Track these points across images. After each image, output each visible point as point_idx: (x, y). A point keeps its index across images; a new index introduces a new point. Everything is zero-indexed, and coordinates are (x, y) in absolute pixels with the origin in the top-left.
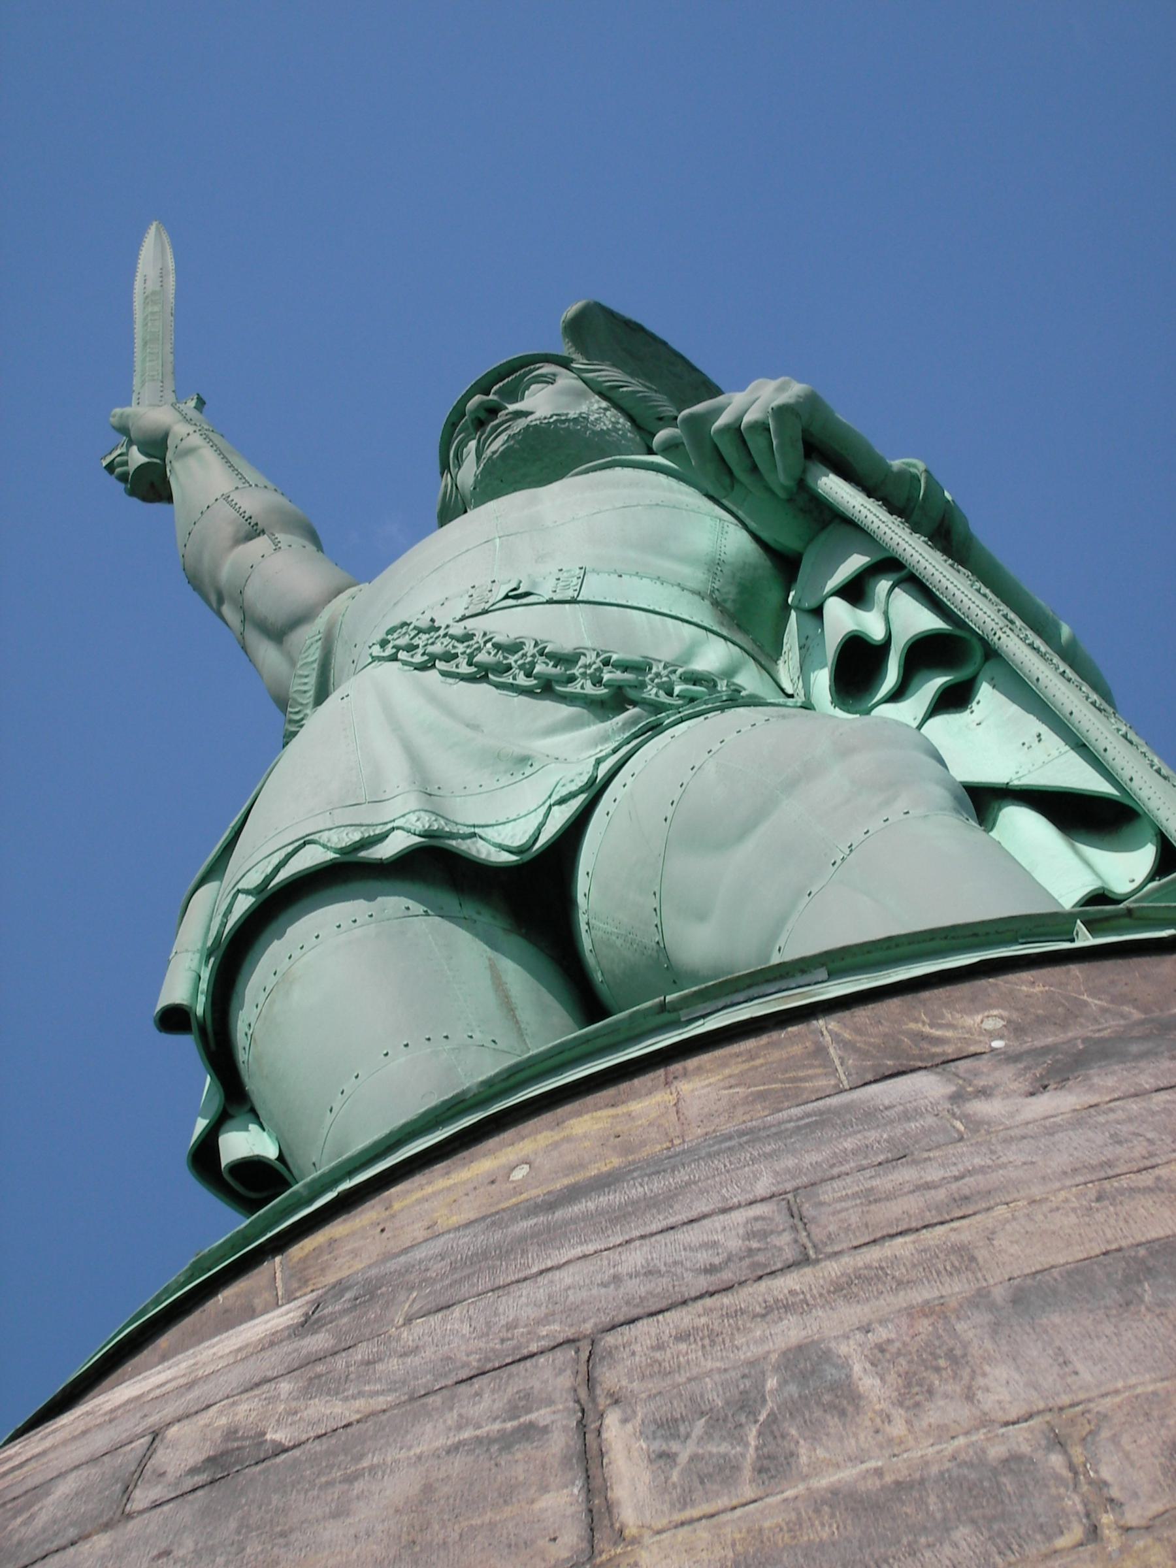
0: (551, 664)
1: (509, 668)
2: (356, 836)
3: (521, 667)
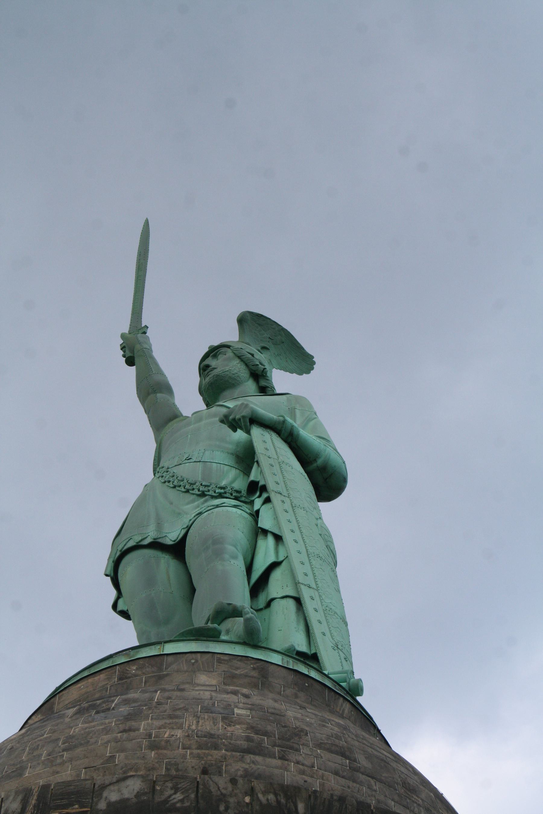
0: (189, 485)
2: (140, 539)
3: (183, 486)
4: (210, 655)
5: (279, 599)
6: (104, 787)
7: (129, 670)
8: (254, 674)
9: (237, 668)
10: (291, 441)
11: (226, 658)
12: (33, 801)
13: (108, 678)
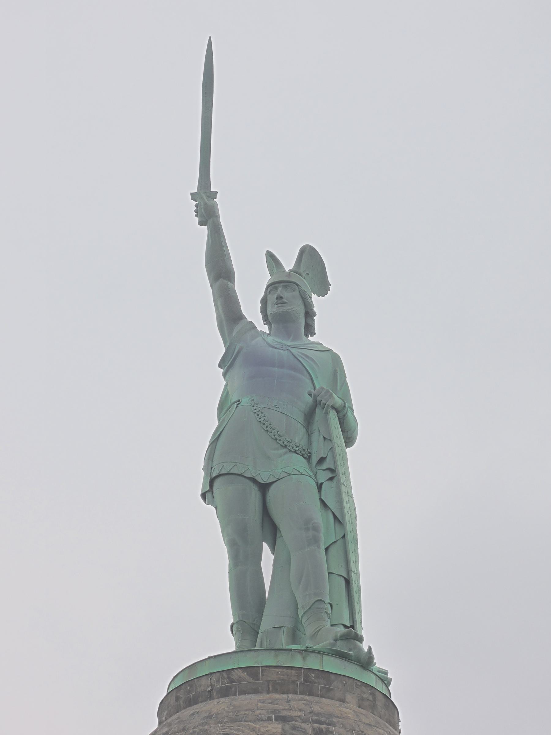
1: (271, 433)
4: (352, 679)
5: (336, 575)
7: (310, 675)
8: (371, 698)
9: (364, 693)
10: (342, 418)
11: (359, 683)
13: (297, 675)
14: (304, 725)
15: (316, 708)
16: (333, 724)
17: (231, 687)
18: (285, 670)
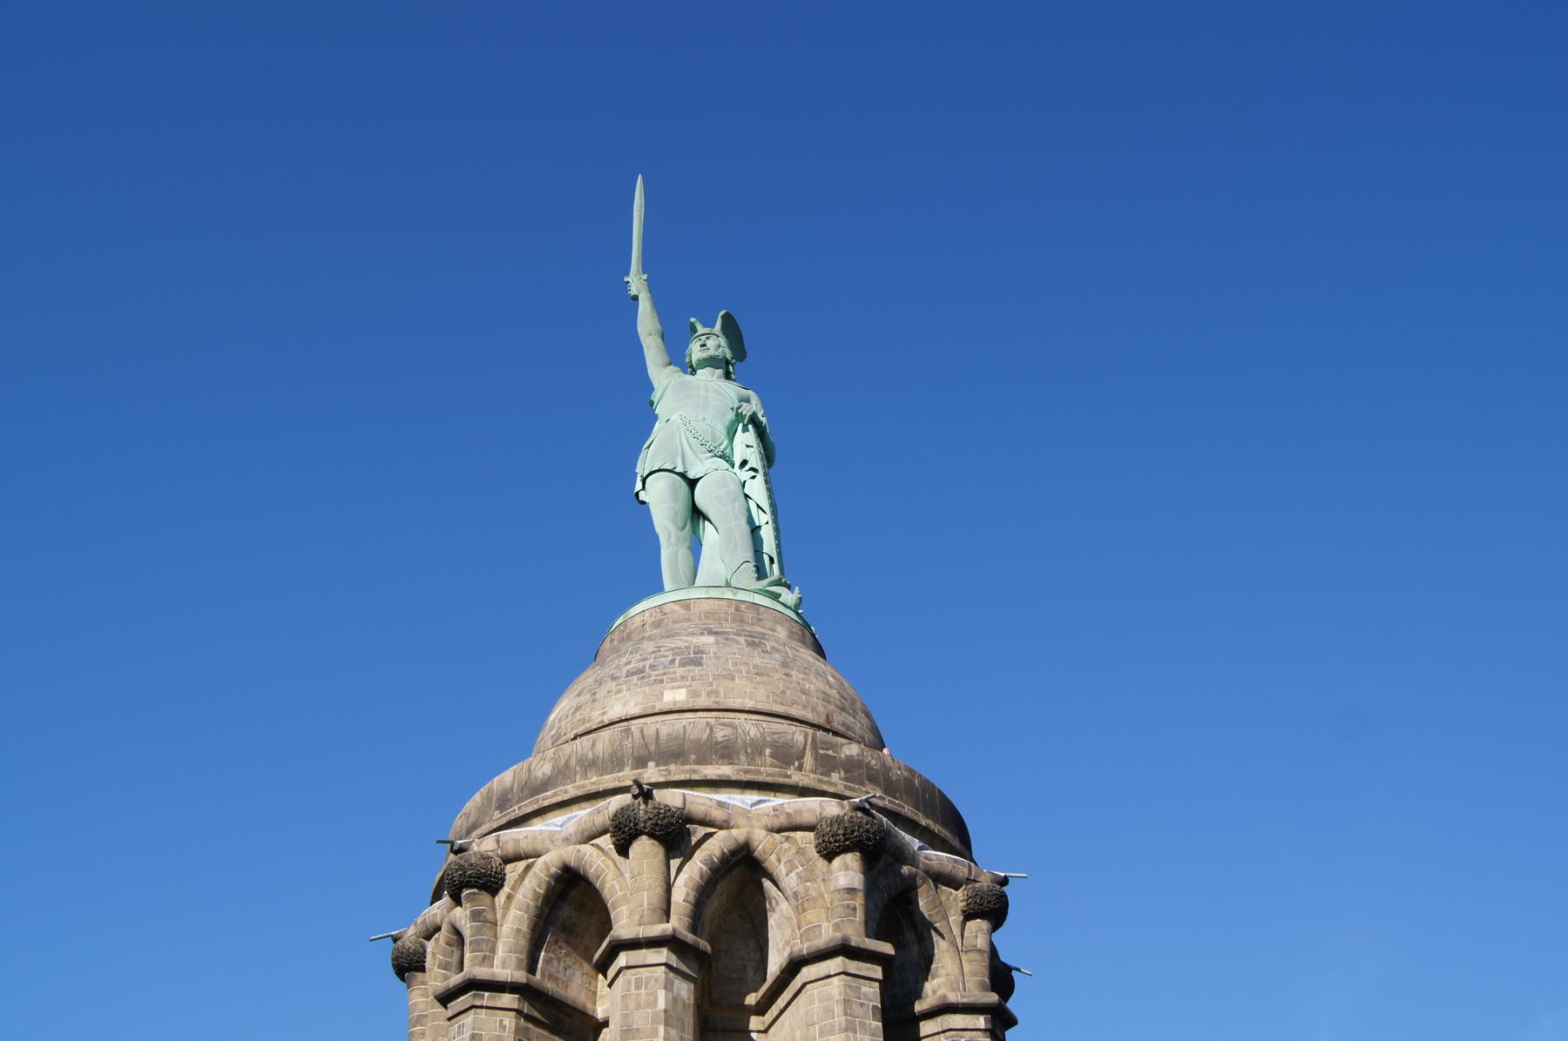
6: (842, 745)
8: (800, 633)
12: (810, 740)
14: (736, 637)
15: (749, 629)
16: (767, 640)
17: (663, 620)
18: (716, 602)
